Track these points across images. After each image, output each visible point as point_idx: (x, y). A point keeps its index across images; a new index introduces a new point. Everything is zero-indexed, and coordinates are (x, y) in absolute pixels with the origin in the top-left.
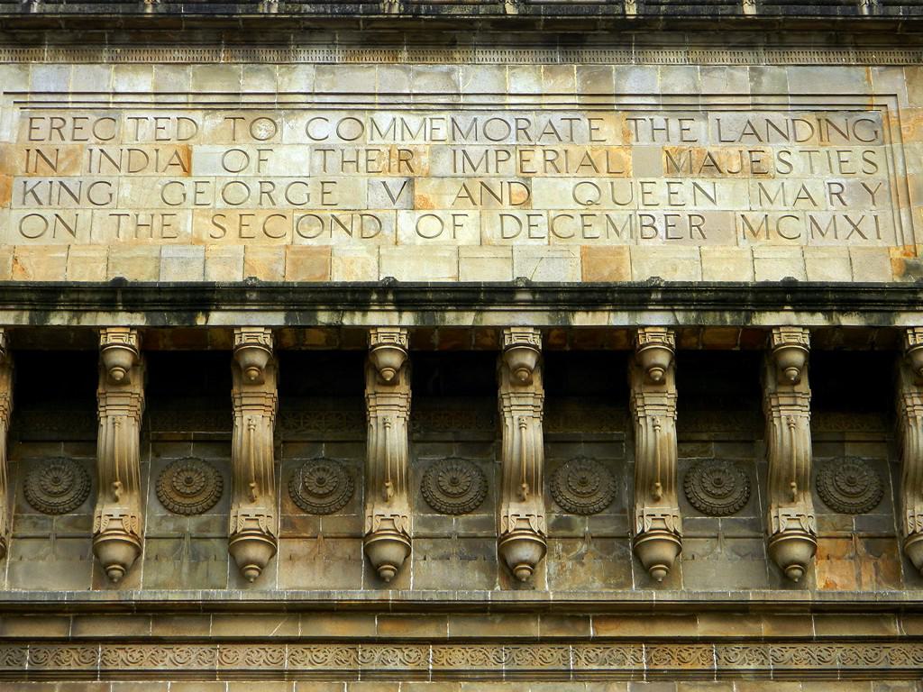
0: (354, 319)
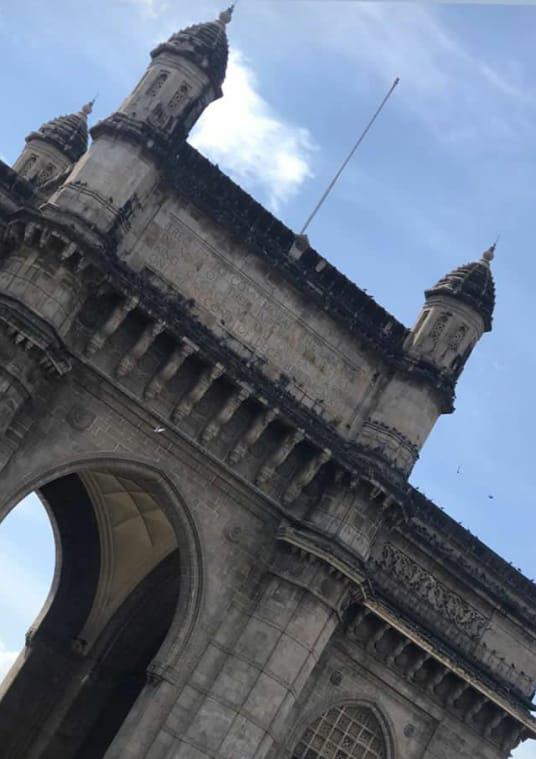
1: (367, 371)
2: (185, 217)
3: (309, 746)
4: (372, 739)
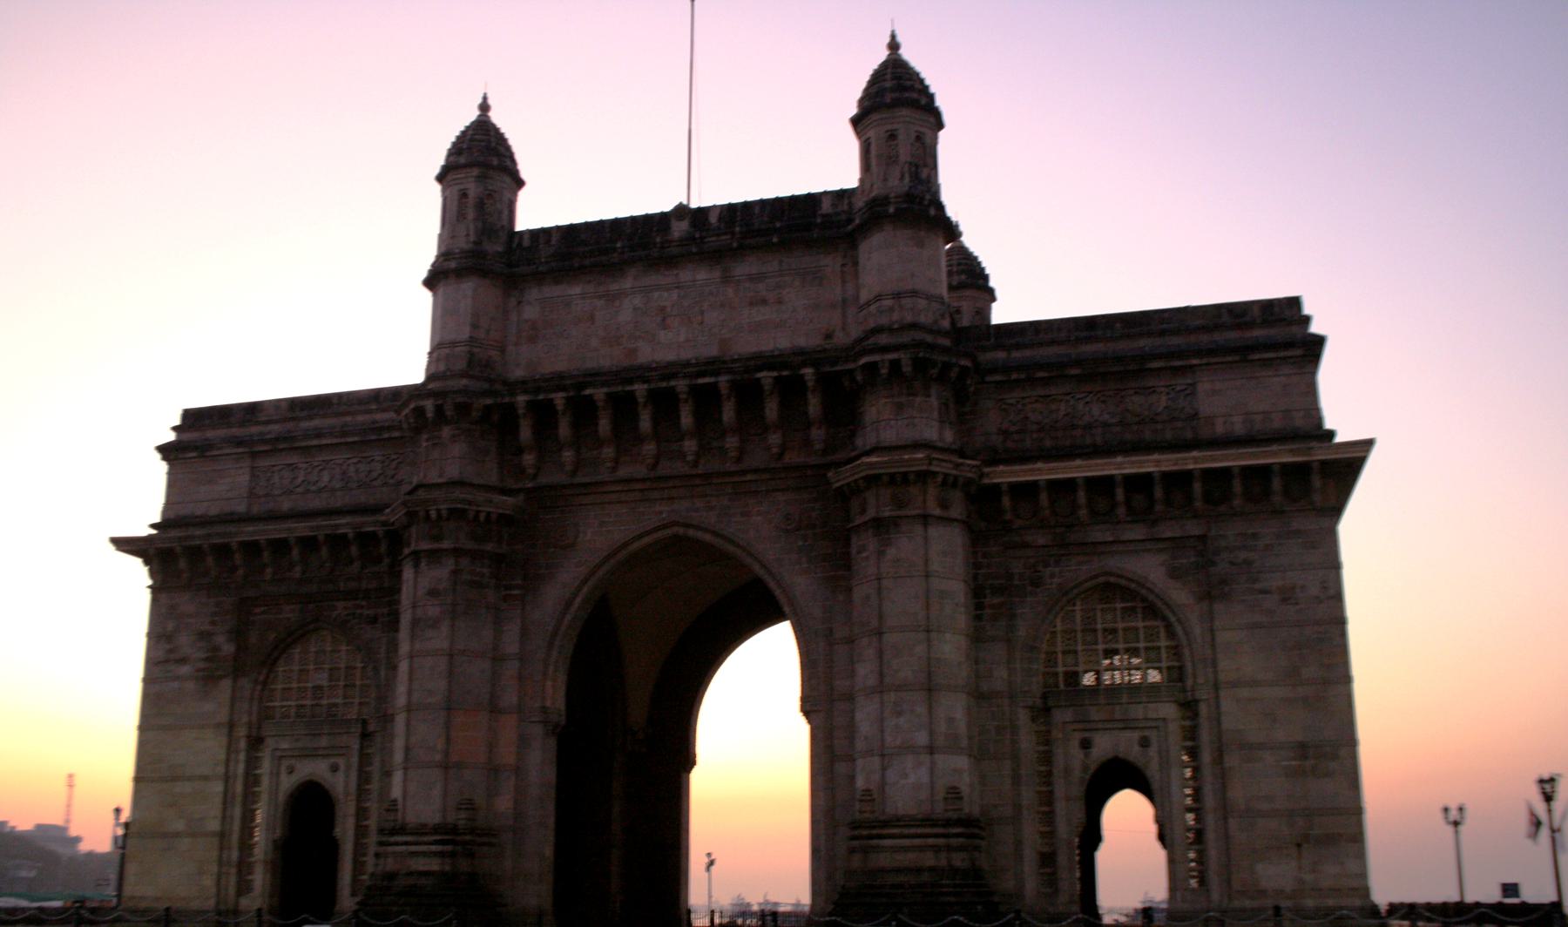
0: (628, 388)
1: (830, 263)
2: (552, 291)
3: (1061, 669)
4: (1139, 610)
